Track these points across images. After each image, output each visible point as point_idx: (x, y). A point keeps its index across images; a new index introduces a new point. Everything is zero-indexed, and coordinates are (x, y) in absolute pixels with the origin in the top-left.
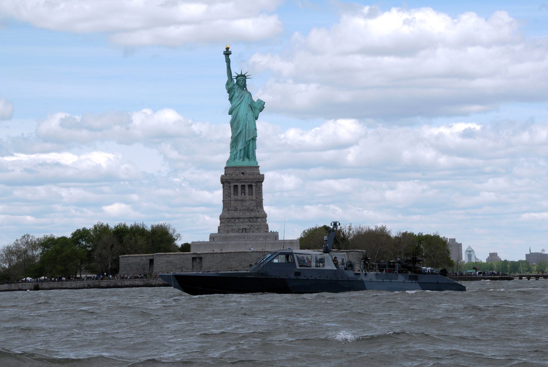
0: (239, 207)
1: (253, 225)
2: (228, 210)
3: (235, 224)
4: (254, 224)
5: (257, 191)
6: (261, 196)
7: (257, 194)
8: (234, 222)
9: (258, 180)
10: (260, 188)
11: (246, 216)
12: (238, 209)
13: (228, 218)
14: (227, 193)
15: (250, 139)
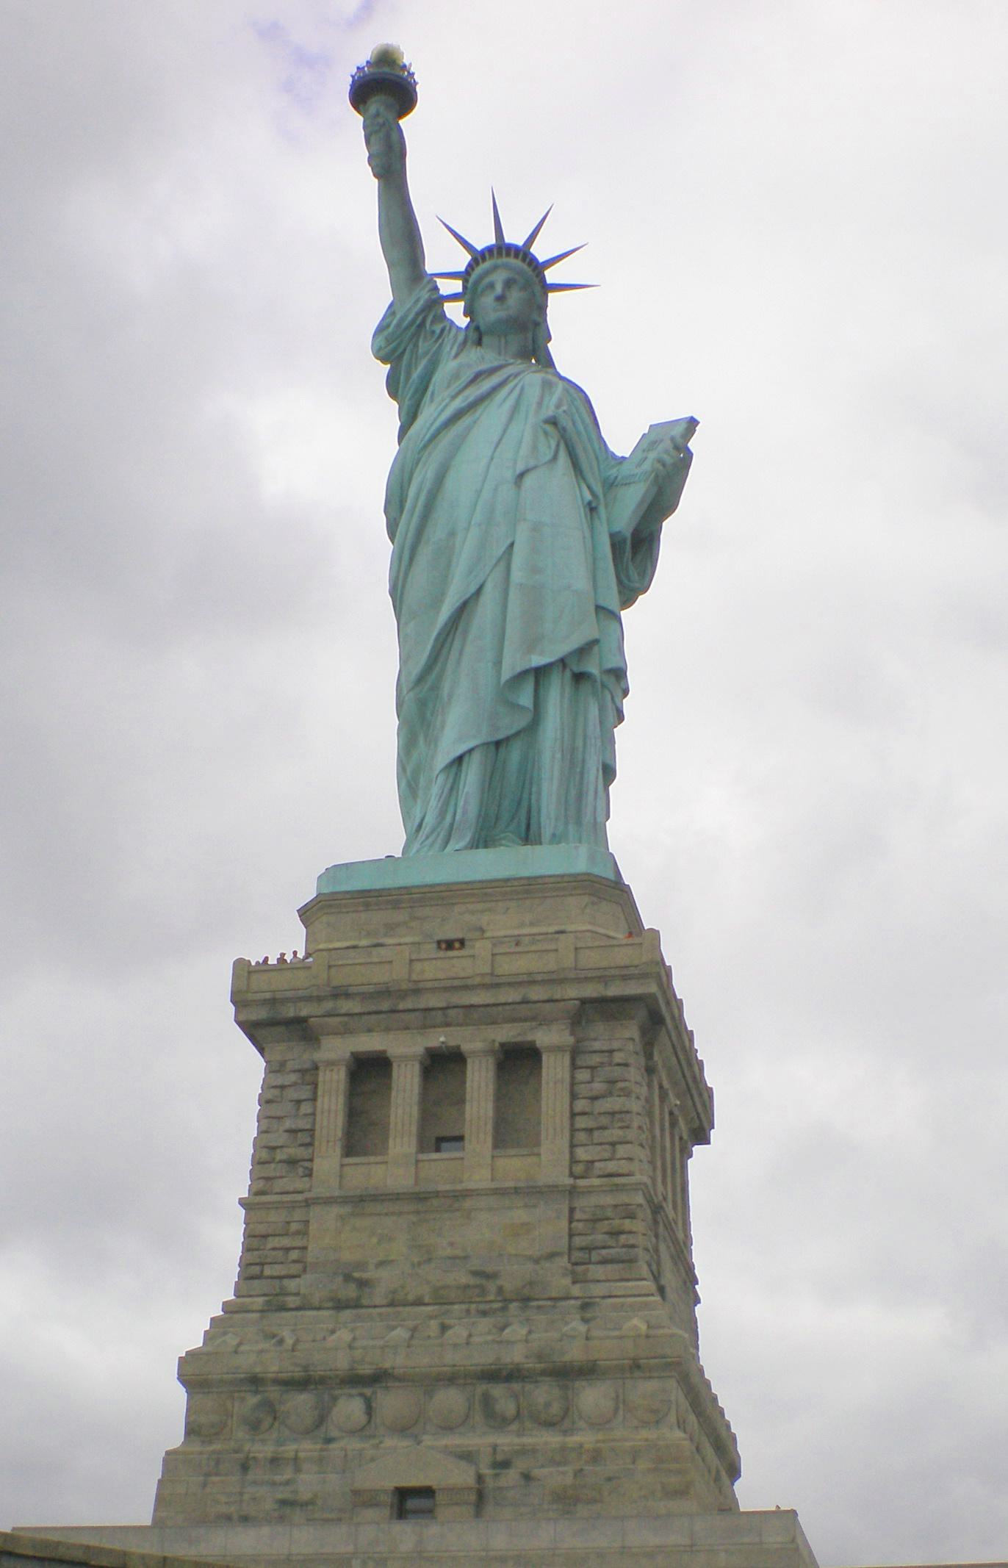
0: (384, 1273)
1: (523, 1451)
2: (276, 1305)
3: (329, 1441)
4: (527, 1440)
5: (581, 1105)
6: (622, 1151)
7: (582, 1137)
8: (321, 1420)
9: (590, 991)
10: (618, 1072)
11: (454, 1358)
12: (379, 1295)
13: (255, 1382)
14: (280, 1139)
15: (537, 660)
